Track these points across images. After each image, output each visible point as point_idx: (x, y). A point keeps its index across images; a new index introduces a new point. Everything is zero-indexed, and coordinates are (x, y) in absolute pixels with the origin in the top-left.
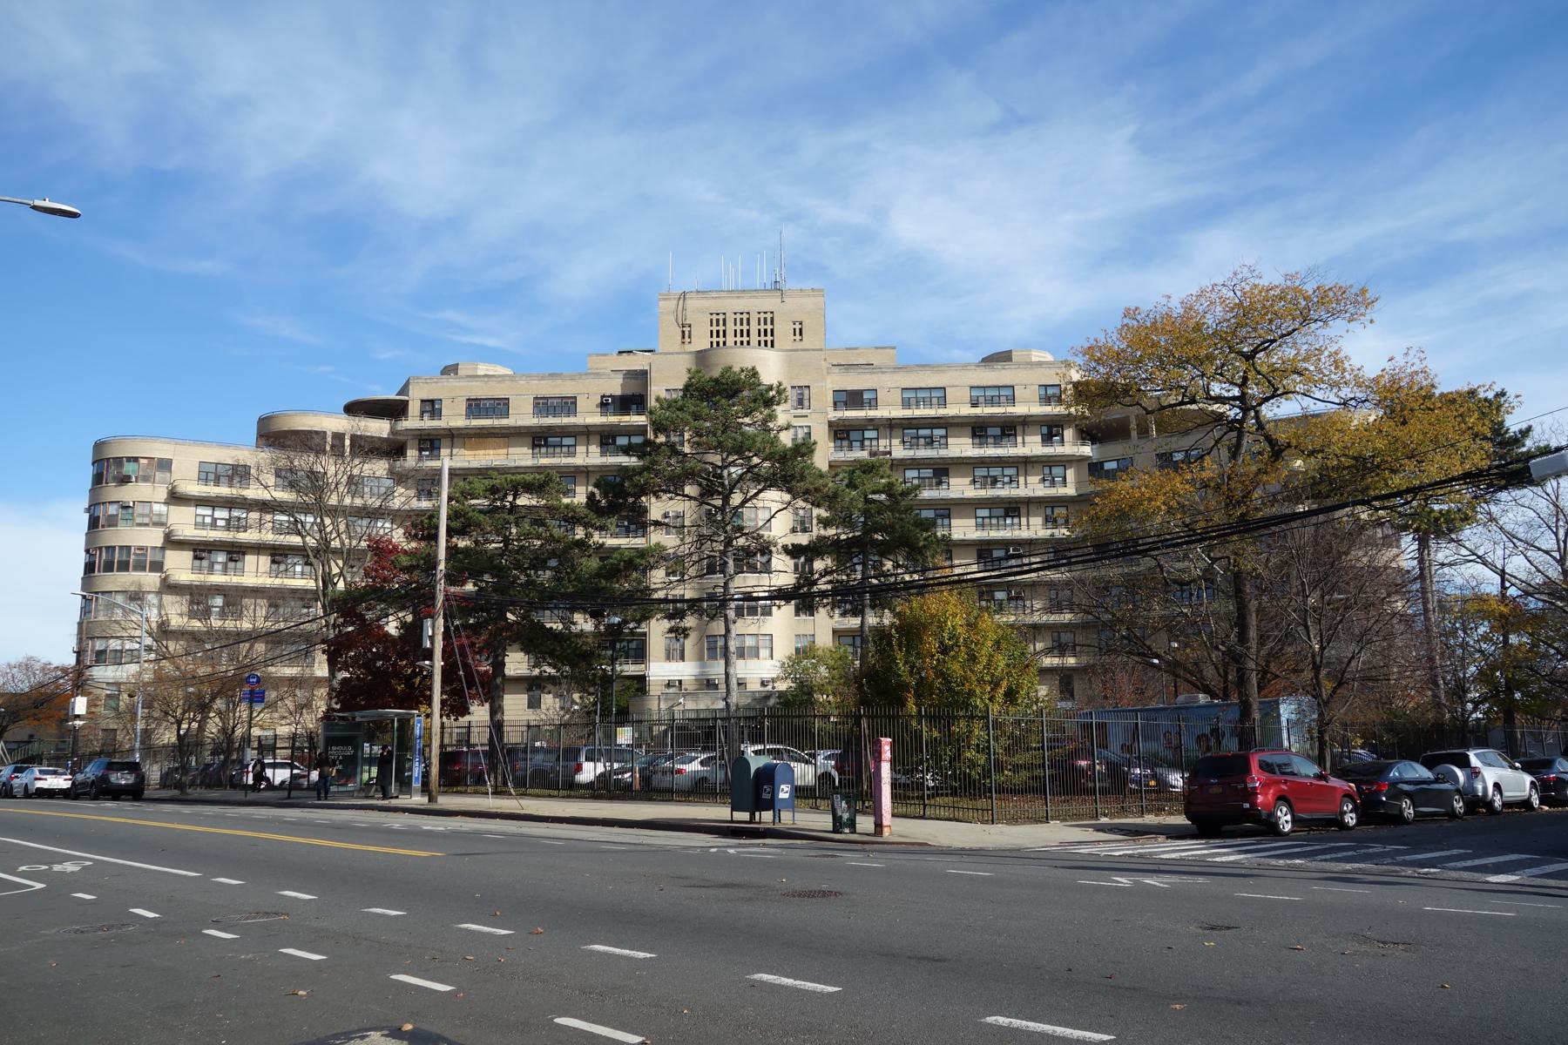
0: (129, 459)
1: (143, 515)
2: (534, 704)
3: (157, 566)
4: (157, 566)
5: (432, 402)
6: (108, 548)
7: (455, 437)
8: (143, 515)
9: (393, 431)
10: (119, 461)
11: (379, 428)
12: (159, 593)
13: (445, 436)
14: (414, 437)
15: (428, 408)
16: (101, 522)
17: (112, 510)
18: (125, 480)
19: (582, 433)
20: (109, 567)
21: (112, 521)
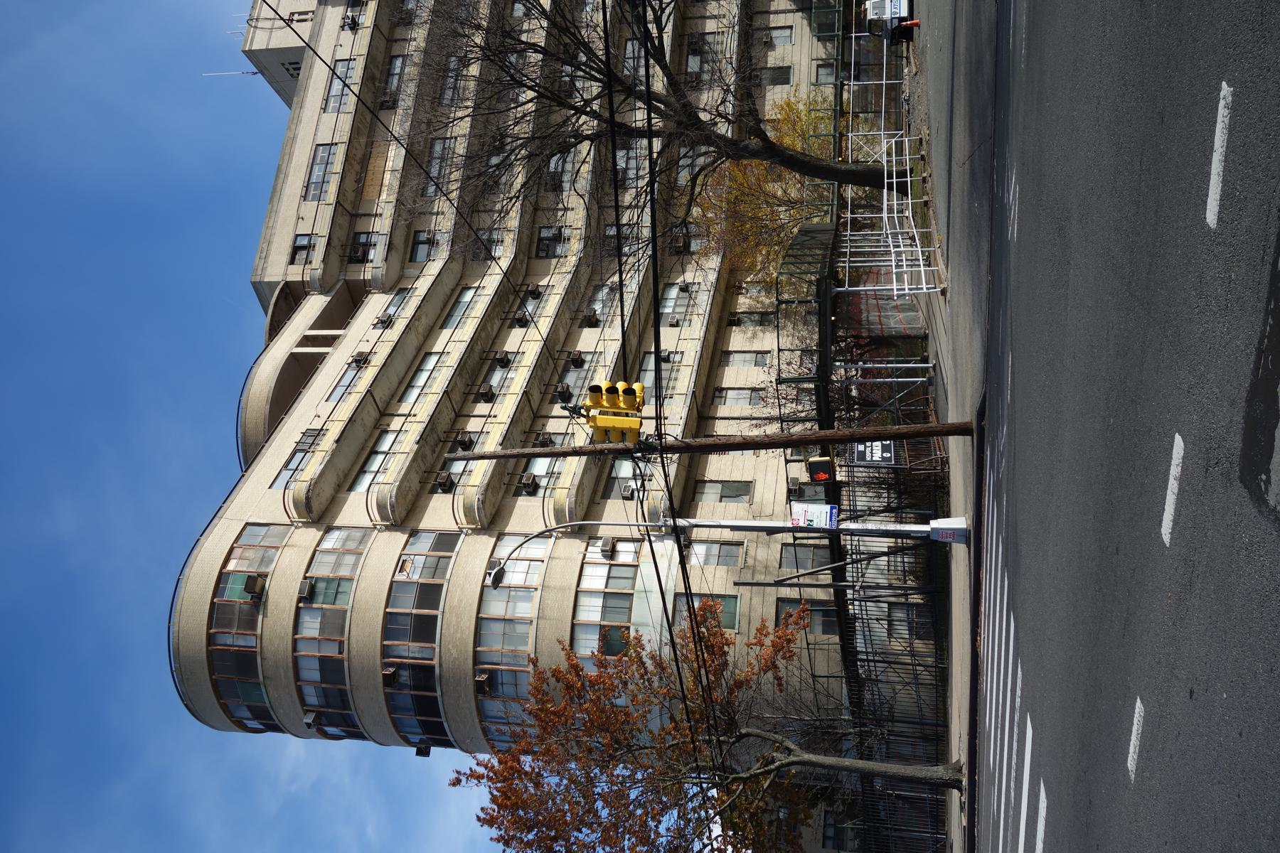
0: (217, 590)
1: (338, 565)
2: (782, 75)
3: (446, 541)
4: (446, 541)
5: (296, 250)
6: (387, 633)
7: (351, 210)
8: (338, 565)
9: (324, 291)
10: (218, 614)
11: (314, 305)
12: (500, 536)
13: (352, 225)
14: (343, 269)
15: (303, 254)
16: (331, 651)
17: (311, 627)
18: (256, 587)
19: (389, 49)
20: (425, 629)
21: (336, 624)
